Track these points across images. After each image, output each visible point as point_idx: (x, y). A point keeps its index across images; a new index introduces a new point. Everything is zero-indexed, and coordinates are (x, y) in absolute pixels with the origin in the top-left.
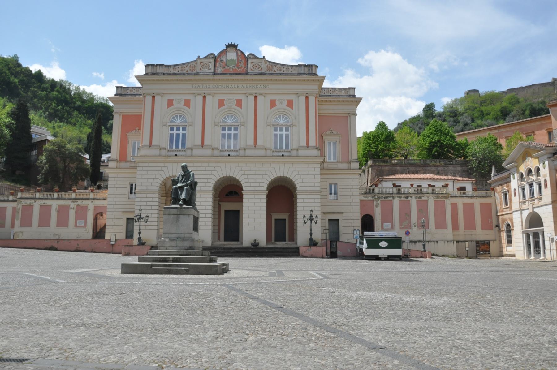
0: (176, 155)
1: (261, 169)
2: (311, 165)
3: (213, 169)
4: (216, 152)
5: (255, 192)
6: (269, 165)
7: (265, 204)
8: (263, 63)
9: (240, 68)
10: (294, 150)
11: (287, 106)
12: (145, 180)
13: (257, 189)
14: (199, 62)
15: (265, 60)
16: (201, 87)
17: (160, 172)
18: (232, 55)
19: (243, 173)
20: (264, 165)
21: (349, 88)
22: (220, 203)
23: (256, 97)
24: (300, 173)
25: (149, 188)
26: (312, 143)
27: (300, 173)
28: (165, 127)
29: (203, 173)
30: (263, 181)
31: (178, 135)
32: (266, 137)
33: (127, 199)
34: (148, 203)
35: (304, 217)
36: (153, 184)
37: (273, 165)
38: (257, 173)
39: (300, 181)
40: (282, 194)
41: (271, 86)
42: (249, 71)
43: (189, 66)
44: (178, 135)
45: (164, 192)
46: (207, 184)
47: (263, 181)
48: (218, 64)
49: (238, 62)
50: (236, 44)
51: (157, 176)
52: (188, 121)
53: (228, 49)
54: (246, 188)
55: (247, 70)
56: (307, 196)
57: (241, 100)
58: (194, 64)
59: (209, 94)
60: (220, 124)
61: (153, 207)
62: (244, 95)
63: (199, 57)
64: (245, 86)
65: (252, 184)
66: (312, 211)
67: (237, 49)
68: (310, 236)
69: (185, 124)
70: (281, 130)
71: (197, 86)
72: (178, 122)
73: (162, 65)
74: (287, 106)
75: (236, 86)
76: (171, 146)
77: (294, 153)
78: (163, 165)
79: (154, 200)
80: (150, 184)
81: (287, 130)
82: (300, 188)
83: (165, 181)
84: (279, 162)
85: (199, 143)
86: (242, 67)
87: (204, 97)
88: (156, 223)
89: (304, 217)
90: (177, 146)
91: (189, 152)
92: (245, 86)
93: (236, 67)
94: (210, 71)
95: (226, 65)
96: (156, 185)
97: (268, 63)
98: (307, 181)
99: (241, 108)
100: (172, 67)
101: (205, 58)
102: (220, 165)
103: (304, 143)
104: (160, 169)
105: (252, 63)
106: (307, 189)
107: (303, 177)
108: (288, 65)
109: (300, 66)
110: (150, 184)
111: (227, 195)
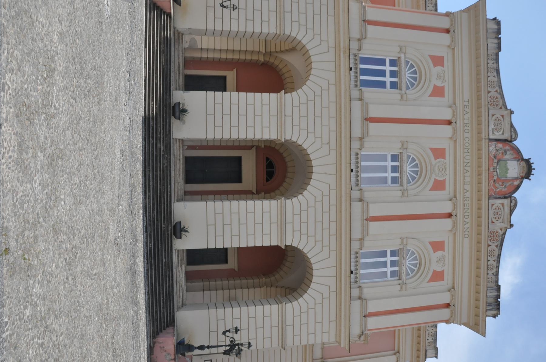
0: (351, 69)
1: (326, 232)
2: (333, 325)
3: (325, 140)
4: (356, 145)
5: (282, 224)
6: (333, 247)
7: (259, 244)
8: (503, 225)
9: (494, 186)
10: (361, 292)
11: (435, 272)
12: (302, 10)
13: (289, 227)
14: (505, 113)
15: (506, 229)
16: (466, 116)
17: (317, 37)
18: (514, 169)
19: (319, 198)
20: (333, 238)
21: (436, 349)
22: (254, 149)
23: (450, 215)
24: (318, 307)
25: (288, 16)
26: (373, 323)
27: (318, 307)
28: (398, 49)
29: (318, 120)
30: (304, 237)
31: (382, 73)
32: (383, 236)
34: (257, 14)
35: (237, 330)
36: (295, 25)
37: (333, 254)
38: (319, 225)
39: (304, 309)
40: (275, 270)
41: (467, 241)
43: (496, 95)
44: (382, 73)
45: (273, 50)
46: (296, 129)
47: (304, 237)
48: (500, 145)
50: (531, 177)
51: (310, 32)
52: (408, 92)
53: (523, 163)
54: (291, 205)
56: (275, 323)
57: (444, 189)
58: (501, 104)
59: (455, 132)
60: (404, 152)
61: (250, 24)
62: (452, 194)
64: (468, 195)
65: (297, 218)
66: (249, 345)
67: (523, 178)
68: (196, 345)
69: (404, 87)
70: (393, 264)
71: (468, 110)
72: (406, 75)
73: (499, 48)
74: (435, 272)
75: (468, 179)
76: (365, 61)
77: (355, 292)
78: (332, 43)
79: (265, 25)
80: (295, 18)
81: (393, 274)
82: (293, 308)
83: (298, 48)
84: (338, 266)
85: (373, 114)
86: (496, 188)
87: (449, 123)
88: (218, 28)
89: (237, 330)
90: (365, 72)
91: (355, 93)
92: (468, 195)
93: (495, 178)
94: (491, 133)
95: (499, 161)
96: (292, 30)
97: (501, 233)
98: (304, 321)
100: (495, 65)
102: (333, 153)
103: (372, 307)
104: (324, 37)
105: (503, 205)
106: (289, 321)
107: (311, 312)
108: (498, 267)
109: (498, 288)
110: (295, 18)
111: (267, 159)
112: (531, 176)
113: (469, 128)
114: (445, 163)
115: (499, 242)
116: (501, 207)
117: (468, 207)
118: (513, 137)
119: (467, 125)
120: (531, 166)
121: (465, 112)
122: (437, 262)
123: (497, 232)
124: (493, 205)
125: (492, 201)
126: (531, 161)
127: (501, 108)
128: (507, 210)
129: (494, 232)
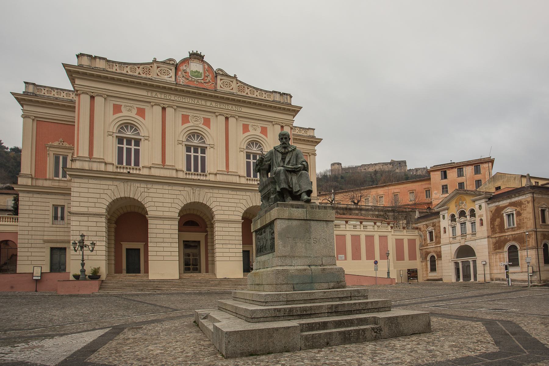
15: (237, 80)
33: (50, 224)
42: (218, 88)
55: (215, 87)
99: (210, 128)
115: (246, 87)
124: (221, 87)
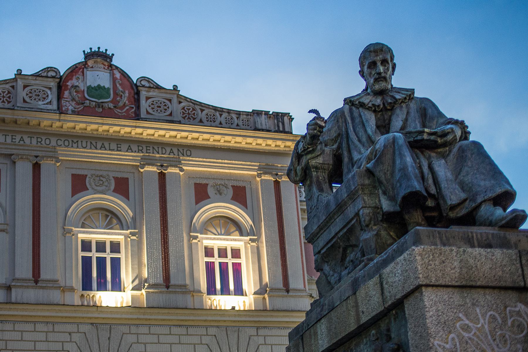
8: (175, 100)
14: (20, 83)
15: (179, 96)
16: (27, 141)
48: (66, 93)
49: (116, 94)
50: (109, 53)
53: (90, 63)
63: (19, 71)
101: (37, 75)
105: (147, 98)
112: (108, 53)
113: (44, 138)
114: (92, 175)
116: (150, 101)
117: (151, 149)
118: (54, 74)
119: (39, 140)
120: (95, 52)
121: (22, 142)
122: (220, 194)
123: (183, 108)
125: (143, 114)
126: (88, 51)
127: (13, 87)
128: (153, 93)
129: (184, 113)
